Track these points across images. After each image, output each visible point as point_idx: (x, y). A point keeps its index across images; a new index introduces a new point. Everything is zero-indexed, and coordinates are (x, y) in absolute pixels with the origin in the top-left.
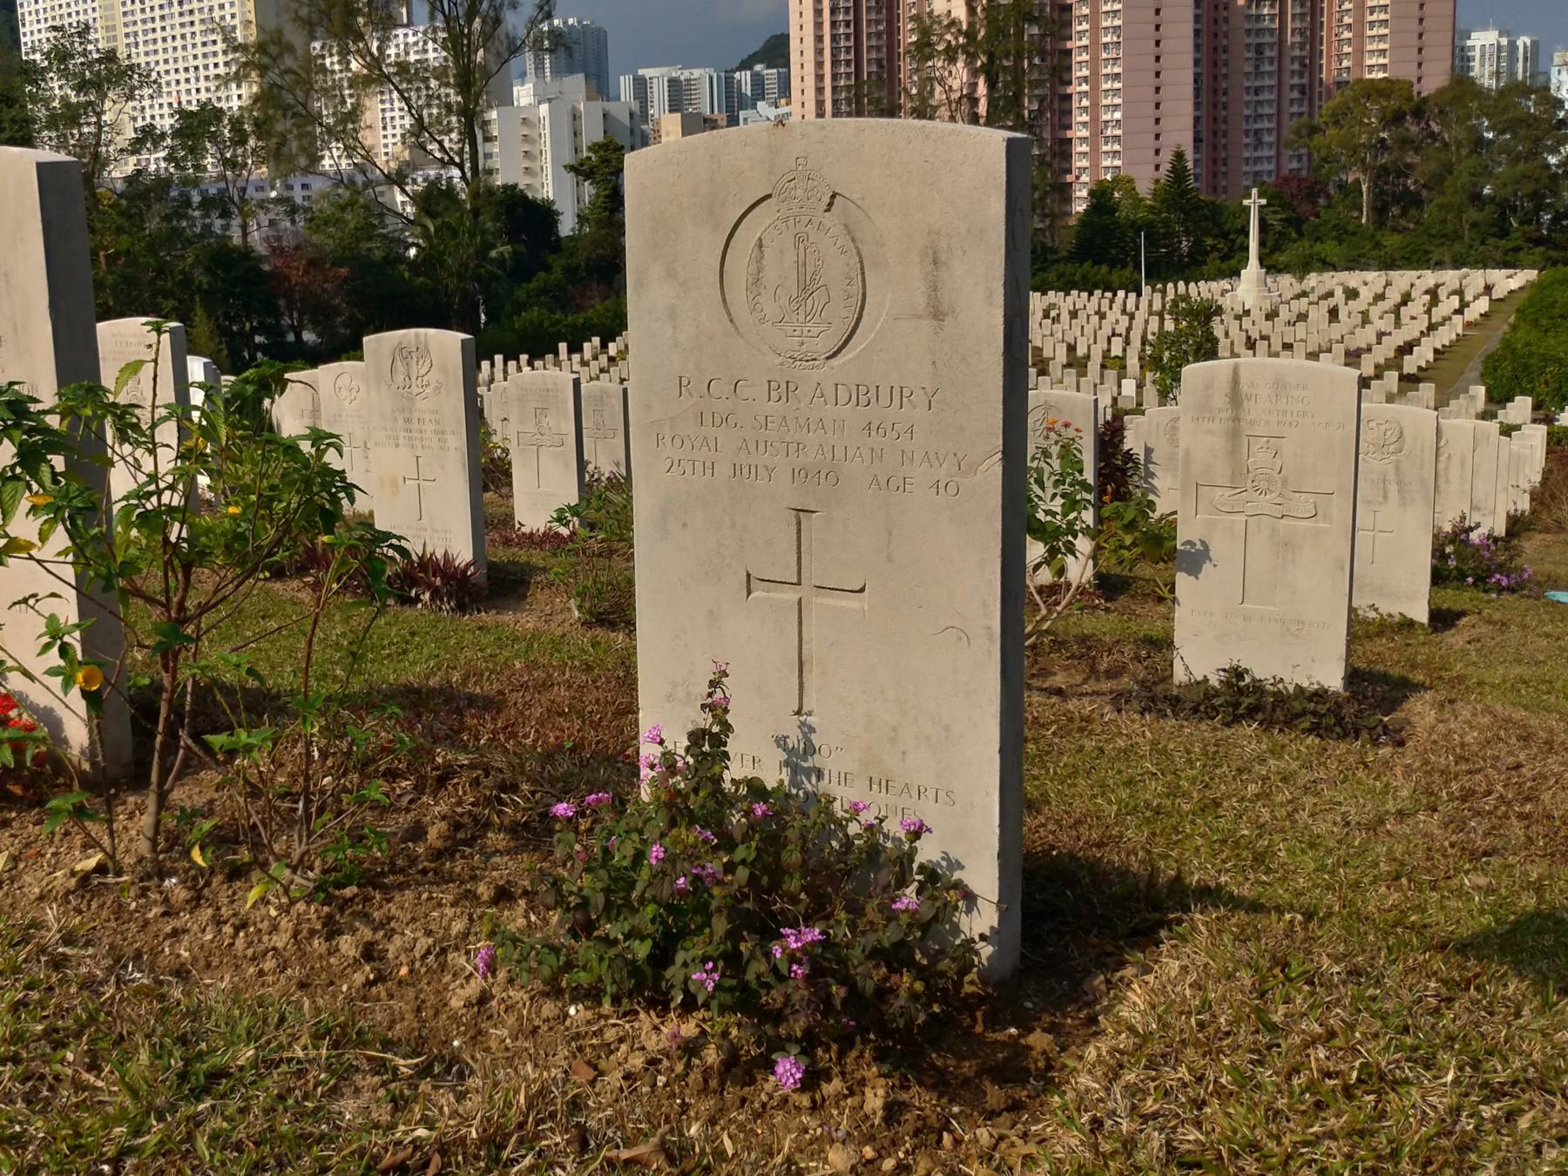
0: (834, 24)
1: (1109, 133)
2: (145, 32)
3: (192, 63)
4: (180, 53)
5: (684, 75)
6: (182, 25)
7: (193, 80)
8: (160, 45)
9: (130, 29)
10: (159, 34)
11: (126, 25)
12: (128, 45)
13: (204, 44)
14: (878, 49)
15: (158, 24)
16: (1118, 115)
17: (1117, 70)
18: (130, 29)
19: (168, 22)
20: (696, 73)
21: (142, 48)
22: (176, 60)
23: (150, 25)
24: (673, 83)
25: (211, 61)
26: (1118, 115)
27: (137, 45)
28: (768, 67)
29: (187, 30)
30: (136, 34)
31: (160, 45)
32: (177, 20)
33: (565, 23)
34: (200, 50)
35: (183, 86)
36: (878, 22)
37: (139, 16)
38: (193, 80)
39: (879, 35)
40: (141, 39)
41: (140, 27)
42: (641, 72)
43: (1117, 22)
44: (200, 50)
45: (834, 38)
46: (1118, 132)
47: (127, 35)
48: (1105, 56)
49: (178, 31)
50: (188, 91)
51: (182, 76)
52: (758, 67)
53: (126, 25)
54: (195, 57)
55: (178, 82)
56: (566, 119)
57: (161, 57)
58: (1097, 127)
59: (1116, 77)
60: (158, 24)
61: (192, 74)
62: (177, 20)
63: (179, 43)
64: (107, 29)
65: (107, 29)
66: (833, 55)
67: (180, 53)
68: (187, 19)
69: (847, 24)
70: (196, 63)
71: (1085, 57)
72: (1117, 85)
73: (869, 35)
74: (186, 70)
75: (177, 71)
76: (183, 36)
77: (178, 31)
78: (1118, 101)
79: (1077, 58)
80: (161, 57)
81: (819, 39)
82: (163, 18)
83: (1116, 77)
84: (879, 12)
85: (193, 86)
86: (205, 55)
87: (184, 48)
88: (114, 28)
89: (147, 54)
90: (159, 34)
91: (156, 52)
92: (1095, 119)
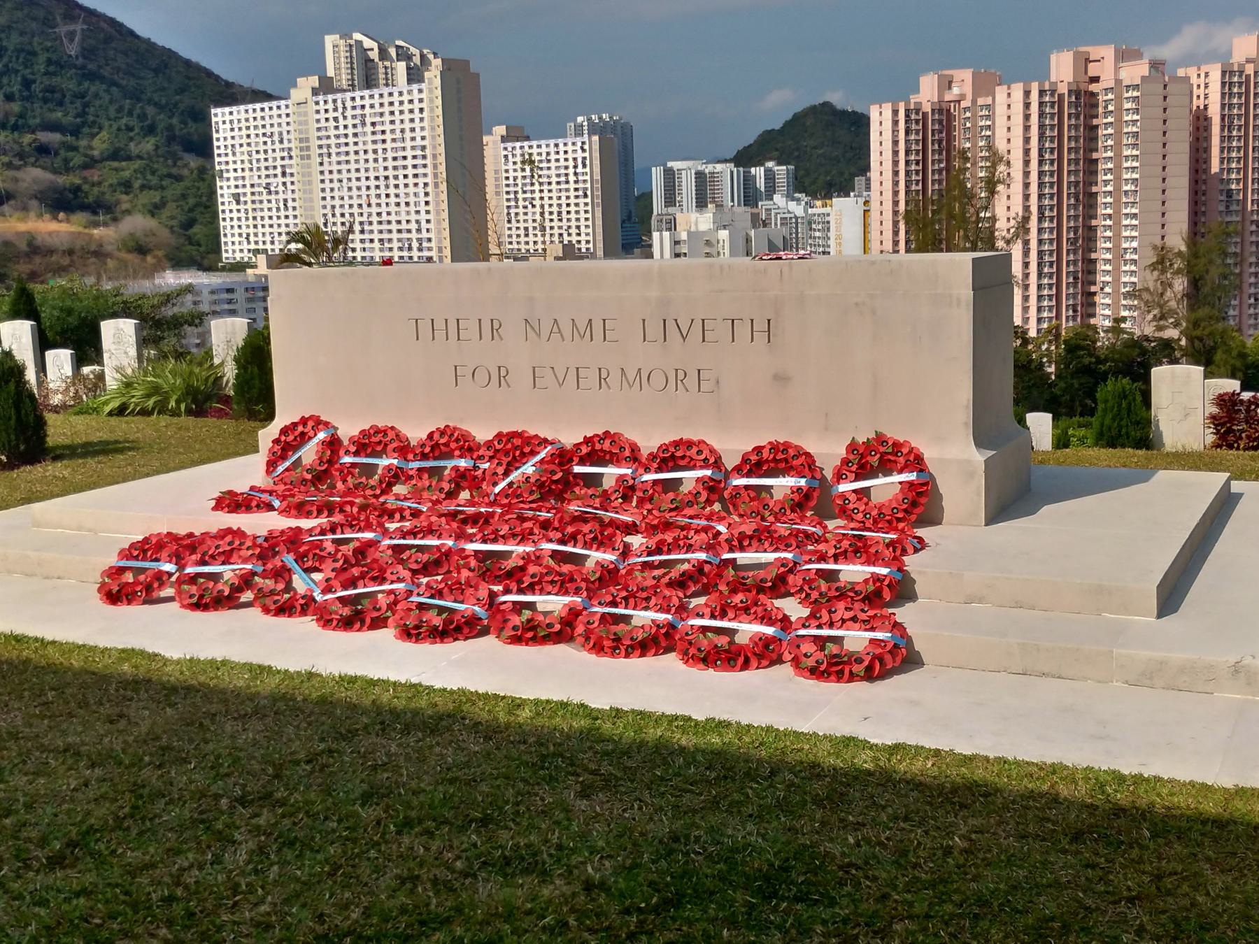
0: (907, 163)
1: (1128, 257)
2: (338, 146)
3: (382, 173)
4: (371, 165)
5: (709, 168)
6: (374, 142)
7: (382, 187)
8: (352, 157)
9: (324, 142)
10: (352, 148)
11: (319, 138)
12: (321, 155)
13: (395, 159)
14: (940, 182)
15: (351, 140)
16: (1135, 244)
17: (1134, 211)
18: (324, 142)
19: (360, 139)
20: (719, 167)
21: (334, 158)
22: (367, 170)
23: (343, 140)
24: (700, 176)
25: (401, 173)
26: (1135, 244)
27: (329, 155)
28: (779, 164)
29: (380, 146)
30: (329, 146)
31: (352, 157)
32: (370, 138)
33: (600, 118)
34: (390, 164)
35: (373, 192)
36: (940, 161)
37: (332, 132)
38: (382, 187)
39: (940, 171)
40: (333, 150)
41: (333, 141)
42: (670, 164)
43: (1135, 176)
44: (390, 164)
45: (908, 173)
46: (1136, 257)
47: (320, 147)
48: (1124, 200)
49: (370, 147)
50: (378, 196)
51: (372, 183)
52: (770, 164)
53: (319, 138)
54: (386, 168)
55: (368, 188)
56: (742, 242)
57: (353, 166)
58: (1119, 254)
59: (1134, 216)
60: (351, 140)
61: (382, 183)
62: (370, 138)
63: (371, 156)
64: (301, 140)
65: (301, 140)
66: (907, 186)
67: (371, 165)
68: (379, 137)
69: (917, 164)
70: (386, 173)
71: (1109, 200)
72: (1134, 222)
73: (933, 171)
74: (377, 178)
75: (367, 178)
76: (375, 151)
77: (370, 147)
78: (1136, 234)
79: (1101, 200)
80: (353, 166)
81: (896, 173)
82: (355, 135)
83: (1134, 216)
84: (940, 154)
85: (383, 191)
86: (395, 168)
87: (376, 160)
88: (307, 140)
89: (339, 163)
90: (352, 148)
91: (348, 162)
92: (1117, 245)
